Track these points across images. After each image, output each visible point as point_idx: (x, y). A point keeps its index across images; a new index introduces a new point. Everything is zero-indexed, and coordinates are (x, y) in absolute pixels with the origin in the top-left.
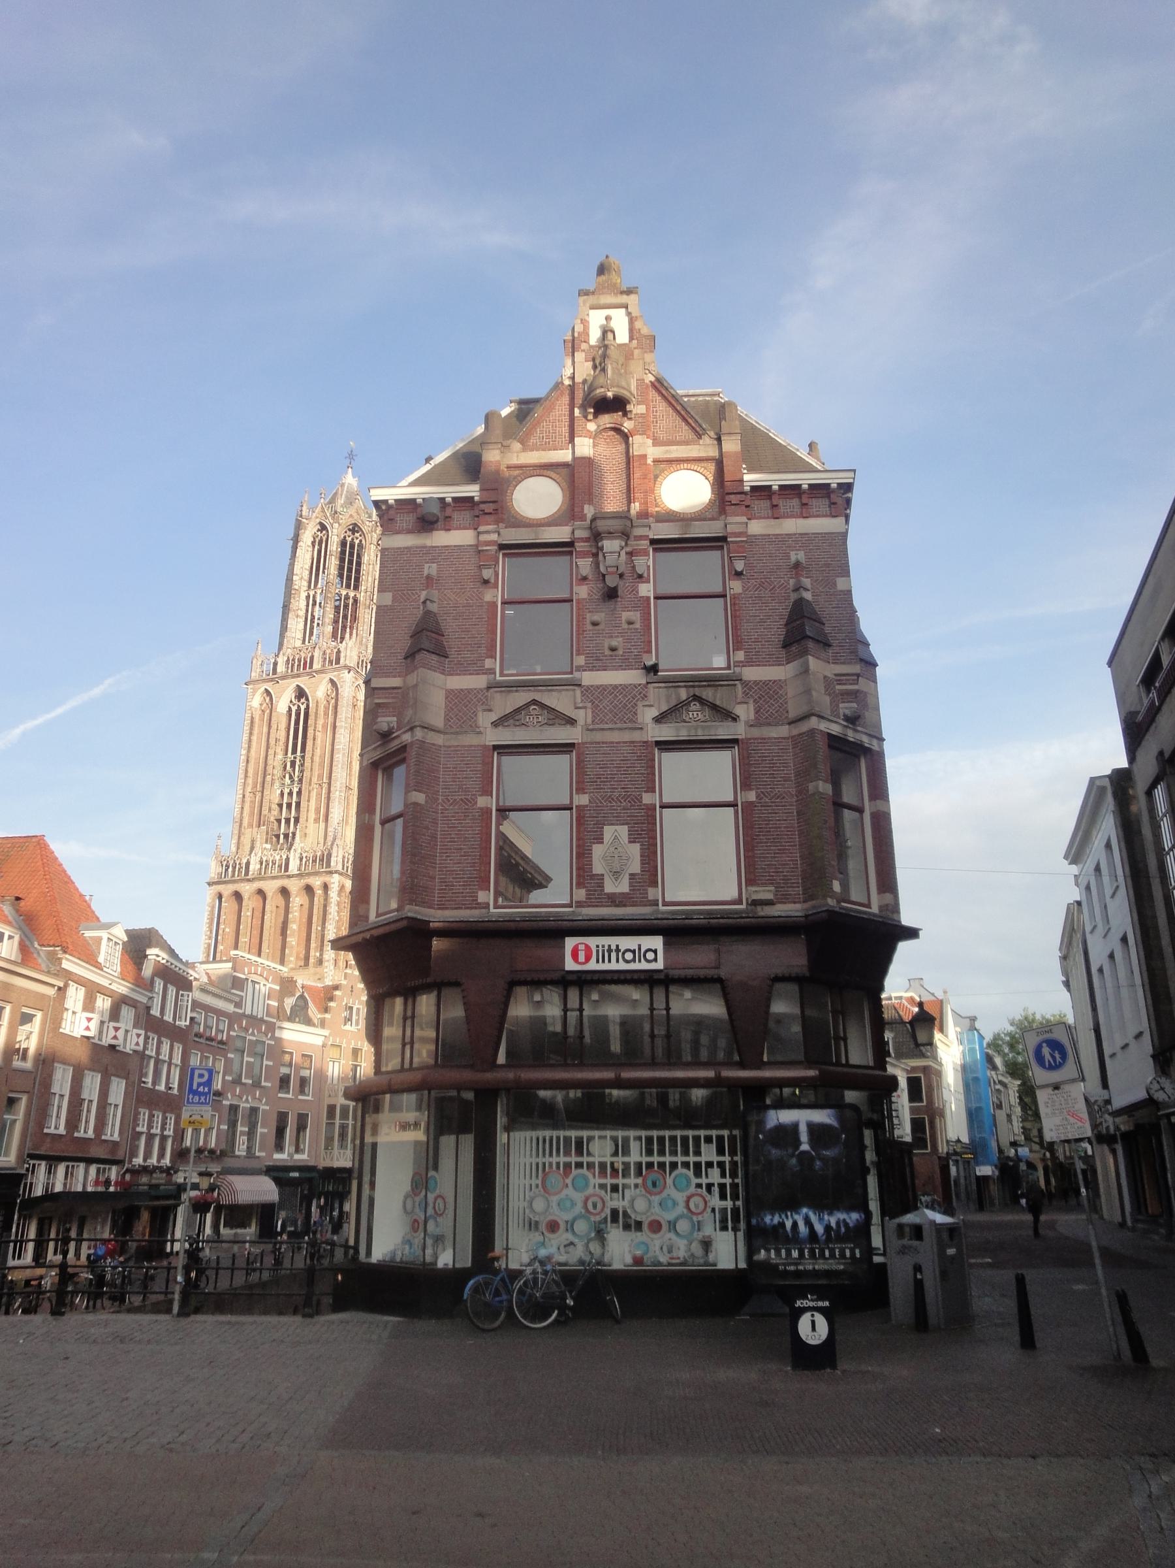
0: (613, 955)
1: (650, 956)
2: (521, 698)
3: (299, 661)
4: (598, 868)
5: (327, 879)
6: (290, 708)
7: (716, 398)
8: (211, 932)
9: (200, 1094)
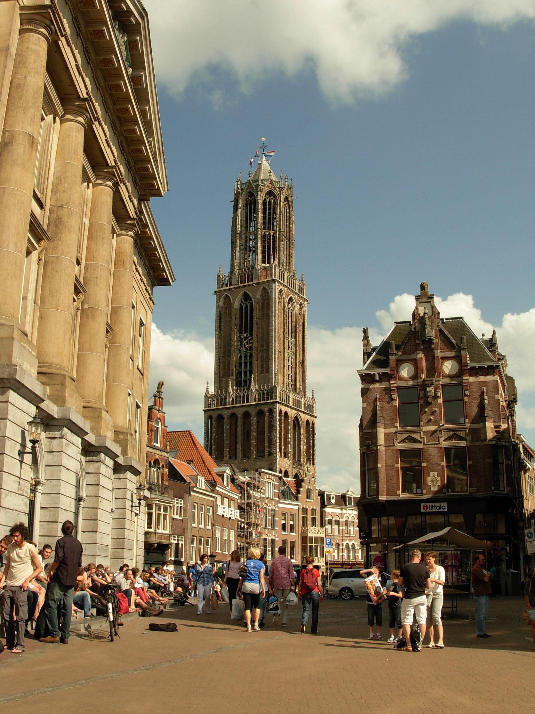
0: (434, 508)
1: (444, 508)
2: (405, 436)
4: (429, 483)
5: (271, 406)
6: (241, 305)
7: (461, 320)
8: (208, 439)
9: (329, 545)
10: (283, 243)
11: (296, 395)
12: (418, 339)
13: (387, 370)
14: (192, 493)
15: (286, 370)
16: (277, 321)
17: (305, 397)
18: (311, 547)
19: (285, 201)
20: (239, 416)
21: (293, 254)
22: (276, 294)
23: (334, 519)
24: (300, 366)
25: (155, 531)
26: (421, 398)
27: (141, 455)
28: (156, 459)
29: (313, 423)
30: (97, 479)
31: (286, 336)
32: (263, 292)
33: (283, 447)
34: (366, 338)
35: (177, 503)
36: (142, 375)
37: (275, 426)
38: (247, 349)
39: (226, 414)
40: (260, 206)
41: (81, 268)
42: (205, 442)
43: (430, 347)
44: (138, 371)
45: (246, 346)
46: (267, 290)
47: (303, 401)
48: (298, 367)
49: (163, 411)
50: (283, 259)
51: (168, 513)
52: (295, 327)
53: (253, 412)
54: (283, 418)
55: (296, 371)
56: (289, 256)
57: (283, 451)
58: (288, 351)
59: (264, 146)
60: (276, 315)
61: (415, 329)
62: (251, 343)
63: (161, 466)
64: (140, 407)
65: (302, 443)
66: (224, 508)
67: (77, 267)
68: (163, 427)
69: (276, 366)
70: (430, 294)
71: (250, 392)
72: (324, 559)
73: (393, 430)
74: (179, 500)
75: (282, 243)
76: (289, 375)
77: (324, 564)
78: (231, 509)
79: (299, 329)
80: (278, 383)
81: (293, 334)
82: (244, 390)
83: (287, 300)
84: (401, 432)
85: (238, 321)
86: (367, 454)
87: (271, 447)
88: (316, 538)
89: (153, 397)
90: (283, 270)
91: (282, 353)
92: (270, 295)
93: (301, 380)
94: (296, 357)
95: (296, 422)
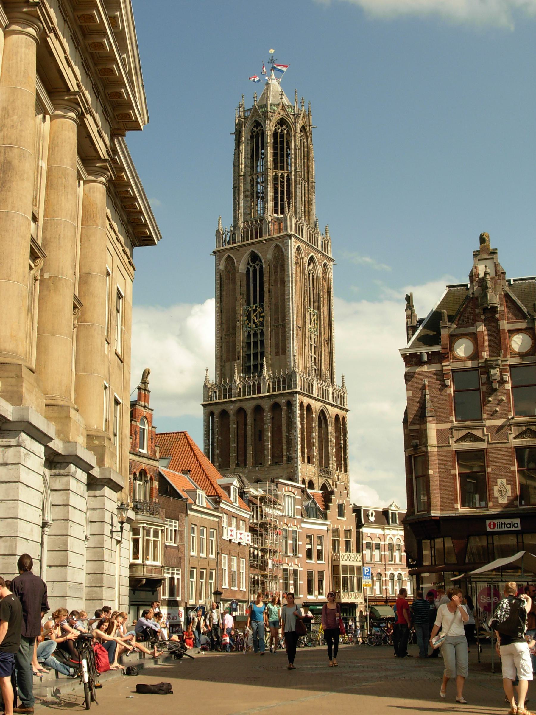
0: (503, 525)
1: (516, 525)
2: (464, 432)
3: (252, 231)
4: (496, 494)
5: (289, 398)
6: (248, 268)
7: (534, 281)
8: (209, 441)
10: (300, 186)
11: (321, 382)
12: (478, 308)
13: (437, 348)
14: (190, 512)
15: (307, 351)
16: (294, 287)
17: (333, 385)
18: (345, 579)
19: (301, 131)
20: (249, 411)
21: (314, 201)
22: (292, 253)
23: (374, 542)
24: (326, 345)
25: (143, 562)
26: (483, 384)
27: (123, 465)
28: (142, 469)
29: (343, 417)
30: (65, 498)
31: (306, 307)
32: (276, 250)
33: (306, 450)
34: (410, 307)
35: (171, 525)
36: (122, 362)
37: (295, 424)
38: (256, 325)
39: (232, 409)
40: (269, 140)
41: (38, 225)
42: (205, 446)
43: (493, 317)
44: (116, 356)
45: (256, 321)
46: (281, 248)
47: (330, 390)
48: (323, 346)
49: (150, 407)
50: (301, 207)
51: (160, 539)
52: (319, 295)
53: (266, 405)
54: (305, 413)
55: (321, 352)
56: (309, 203)
57: (306, 455)
58: (310, 326)
59: (272, 60)
60: (294, 279)
61: (473, 294)
62: (262, 317)
63: (149, 479)
64: (120, 403)
65: (330, 444)
66: (231, 531)
67: (33, 225)
68: (150, 428)
69: (294, 346)
70: (492, 247)
71: (262, 380)
72: (362, 594)
73: (447, 426)
74: (173, 521)
75: (299, 186)
76: (311, 356)
77: (362, 601)
78: (240, 532)
79: (324, 297)
80: (298, 367)
81: (316, 304)
82: (254, 377)
83: (307, 260)
84: (458, 428)
85: (245, 288)
86: (414, 457)
87: (291, 450)
88: (352, 568)
89: (137, 390)
90: (300, 221)
91: (302, 328)
92: (285, 254)
93: (327, 363)
94: (320, 333)
95: (322, 418)
